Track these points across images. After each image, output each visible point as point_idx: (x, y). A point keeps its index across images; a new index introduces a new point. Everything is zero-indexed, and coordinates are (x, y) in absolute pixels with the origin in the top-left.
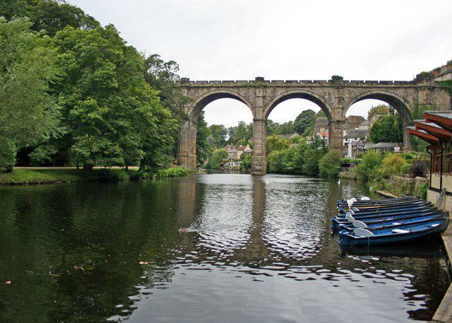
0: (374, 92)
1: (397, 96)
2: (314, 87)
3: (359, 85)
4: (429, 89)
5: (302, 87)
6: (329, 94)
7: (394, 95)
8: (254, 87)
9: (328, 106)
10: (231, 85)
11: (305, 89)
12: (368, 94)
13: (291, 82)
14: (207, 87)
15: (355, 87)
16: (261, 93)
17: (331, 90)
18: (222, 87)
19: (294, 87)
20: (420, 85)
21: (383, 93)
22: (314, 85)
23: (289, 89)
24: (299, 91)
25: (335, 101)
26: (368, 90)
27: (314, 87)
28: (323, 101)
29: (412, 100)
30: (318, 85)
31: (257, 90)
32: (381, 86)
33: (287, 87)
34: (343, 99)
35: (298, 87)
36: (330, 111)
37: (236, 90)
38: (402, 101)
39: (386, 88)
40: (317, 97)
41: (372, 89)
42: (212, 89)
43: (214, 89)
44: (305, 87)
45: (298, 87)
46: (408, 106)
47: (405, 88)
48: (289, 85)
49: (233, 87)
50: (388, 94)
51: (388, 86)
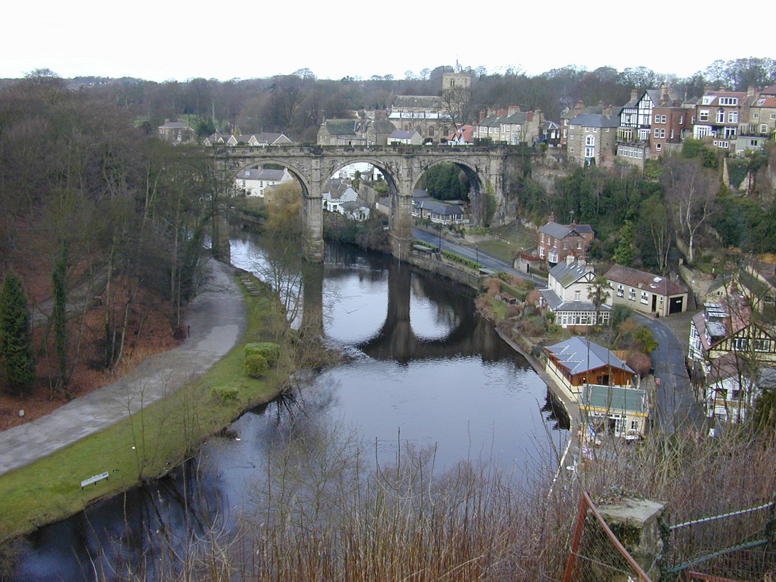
1: (469, 165)
3: (430, 153)
5: (366, 156)
6: (397, 164)
7: (466, 164)
8: (309, 157)
14: (249, 157)
15: (424, 156)
16: (319, 164)
17: (399, 160)
18: (270, 157)
19: (356, 156)
20: (494, 153)
25: (403, 173)
29: (484, 169)
31: (314, 161)
32: (452, 153)
35: (361, 156)
36: (397, 183)
37: (287, 161)
38: (475, 170)
39: (460, 156)
41: (443, 158)
42: (256, 159)
44: (369, 156)
45: (361, 156)
47: (477, 155)
49: (284, 157)
50: (460, 162)
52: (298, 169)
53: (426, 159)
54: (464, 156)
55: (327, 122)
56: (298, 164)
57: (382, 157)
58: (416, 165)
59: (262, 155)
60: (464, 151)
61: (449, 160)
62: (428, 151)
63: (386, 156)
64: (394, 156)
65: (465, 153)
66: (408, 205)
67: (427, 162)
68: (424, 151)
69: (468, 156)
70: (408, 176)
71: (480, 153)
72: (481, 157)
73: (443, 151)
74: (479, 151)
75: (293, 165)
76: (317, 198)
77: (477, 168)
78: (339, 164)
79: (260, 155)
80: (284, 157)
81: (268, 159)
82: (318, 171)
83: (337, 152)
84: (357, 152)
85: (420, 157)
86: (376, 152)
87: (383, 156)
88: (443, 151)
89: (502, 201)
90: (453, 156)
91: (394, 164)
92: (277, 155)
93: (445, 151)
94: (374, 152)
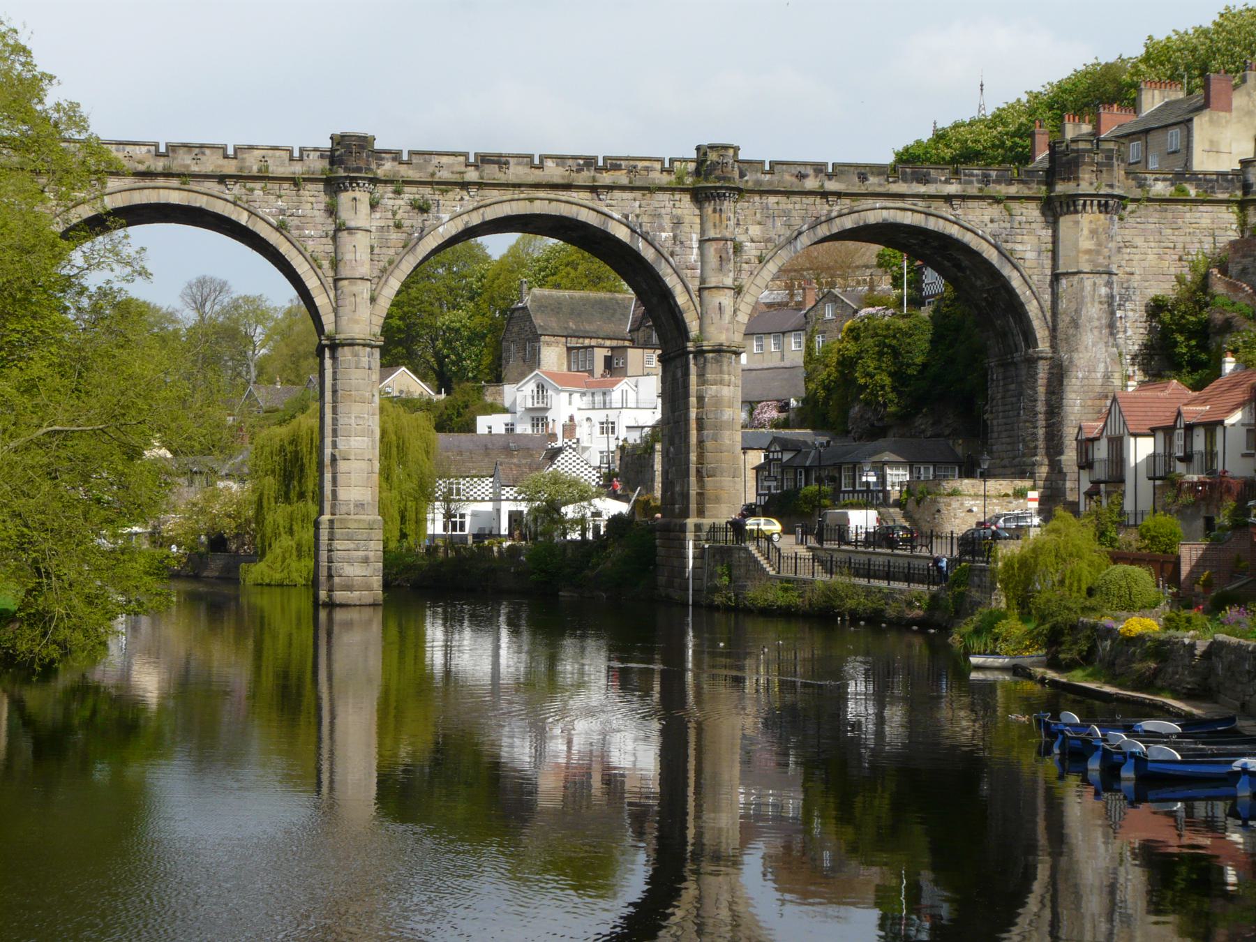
0: (873, 218)
1: (968, 238)
2: (611, 188)
3: (811, 183)
4: (1104, 208)
6: (677, 223)
7: (954, 231)
9: (671, 281)
10: (210, 163)
11: (564, 195)
12: (848, 223)
13: (500, 161)
15: (788, 193)
16: (364, 207)
21: (908, 219)
22: (606, 178)
23: (494, 194)
24: (539, 208)
26: (846, 202)
27: (611, 188)
28: (648, 254)
29: (1031, 255)
30: (622, 178)
33: (480, 185)
34: (738, 249)
35: (537, 186)
36: (681, 299)
38: (991, 255)
40: (622, 233)
43: (127, 182)
44: (567, 187)
45: (537, 186)
46: (1016, 283)
48: (492, 172)
49: (222, 179)
50: (932, 224)
51: (930, 189)
52: (281, 228)
53: (796, 206)
54: (948, 199)
55: (535, 296)
56: (282, 212)
57: (617, 194)
58: (755, 231)
59: (141, 168)
60: (947, 182)
61: (885, 214)
62: (801, 176)
63: (632, 189)
64: (662, 189)
65: (953, 188)
66: (721, 382)
67: (796, 221)
68: (787, 177)
69: (964, 198)
70: (721, 269)
71: (1013, 190)
72: (1016, 207)
73: (863, 178)
74: (1010, 182)
75: (264, 211)
76: (351, 344)
77: (1000, 252)
78: (445, 217)
79: (129, 165)
80: (222, 179)
81: (161, 182)
82: (360, 234)
83: (440, 166)
84: (516, 172)
85: (772, 199)
86: (592, 173)
87: (623, 188)
88: (863, 178)
89: (1107, 377)
90: (901, 196)
91: (667, 222)
92: (195, 169)
93: (872, 180)
94: (585, 173)
